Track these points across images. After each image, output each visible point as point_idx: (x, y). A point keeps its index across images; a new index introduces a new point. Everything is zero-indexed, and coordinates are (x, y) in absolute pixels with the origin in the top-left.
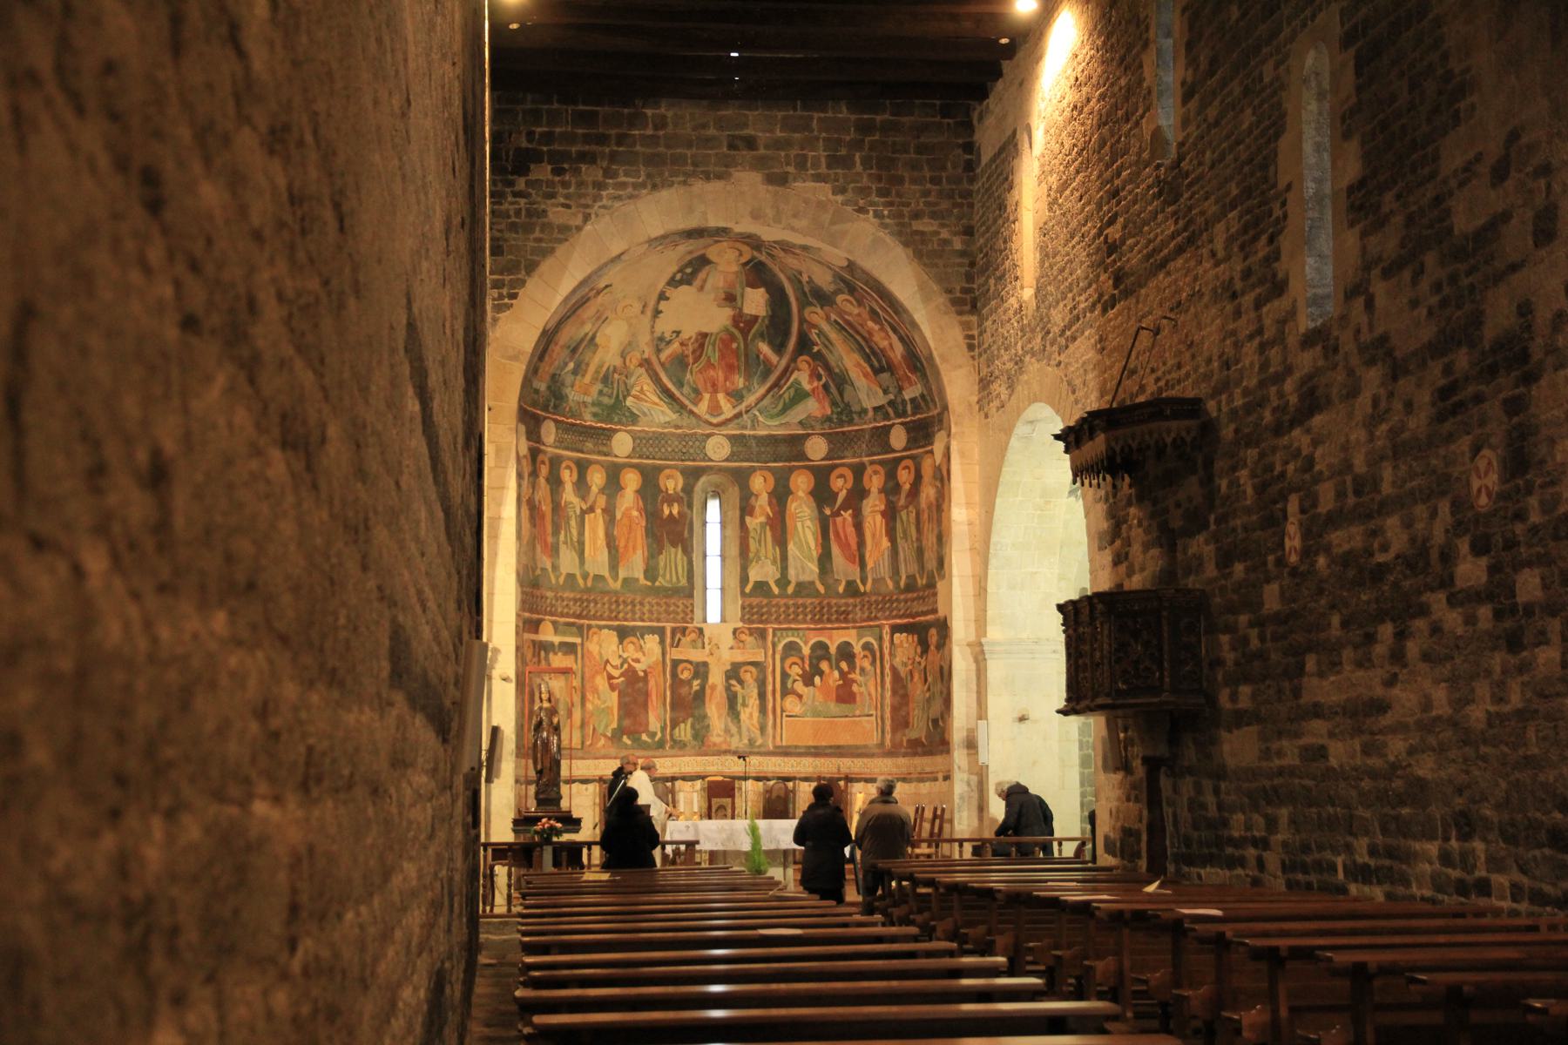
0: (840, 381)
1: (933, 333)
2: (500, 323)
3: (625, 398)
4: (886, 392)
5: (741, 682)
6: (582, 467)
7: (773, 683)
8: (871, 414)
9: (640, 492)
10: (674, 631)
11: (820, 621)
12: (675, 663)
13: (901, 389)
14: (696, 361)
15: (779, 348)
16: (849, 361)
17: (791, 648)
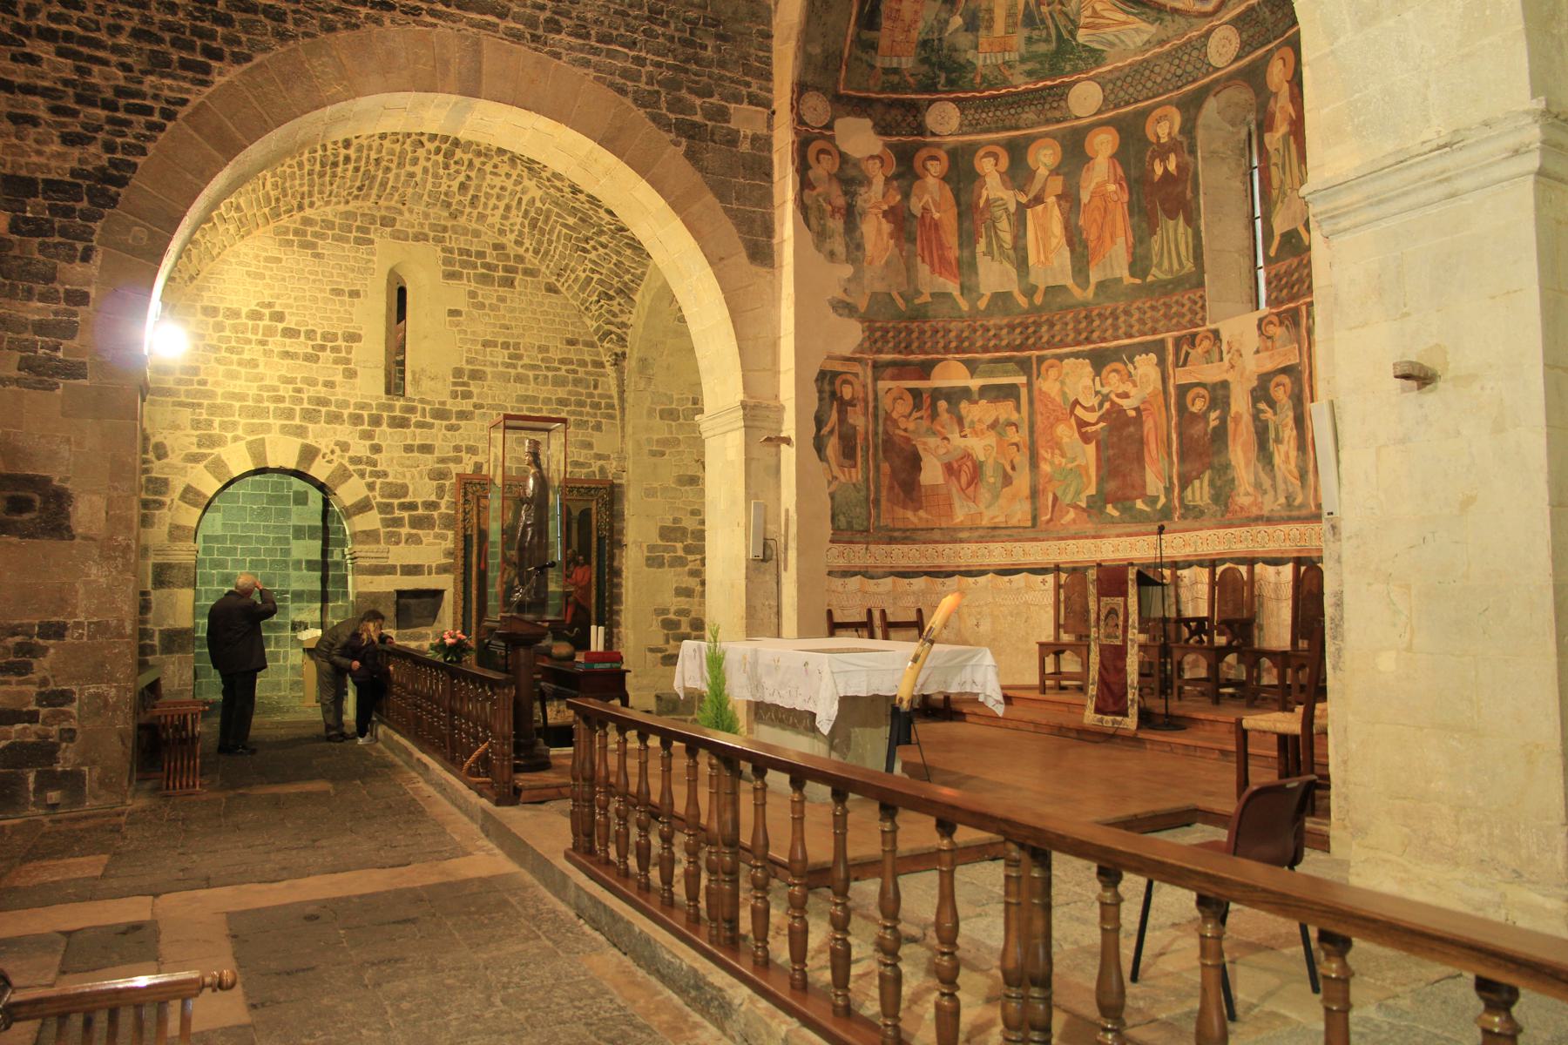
3: (1073, 34)
5: (1272, 404)
6: (1017, 152)
9: (1119, 156)
10: (1178, 343)
12: (1183, 390)
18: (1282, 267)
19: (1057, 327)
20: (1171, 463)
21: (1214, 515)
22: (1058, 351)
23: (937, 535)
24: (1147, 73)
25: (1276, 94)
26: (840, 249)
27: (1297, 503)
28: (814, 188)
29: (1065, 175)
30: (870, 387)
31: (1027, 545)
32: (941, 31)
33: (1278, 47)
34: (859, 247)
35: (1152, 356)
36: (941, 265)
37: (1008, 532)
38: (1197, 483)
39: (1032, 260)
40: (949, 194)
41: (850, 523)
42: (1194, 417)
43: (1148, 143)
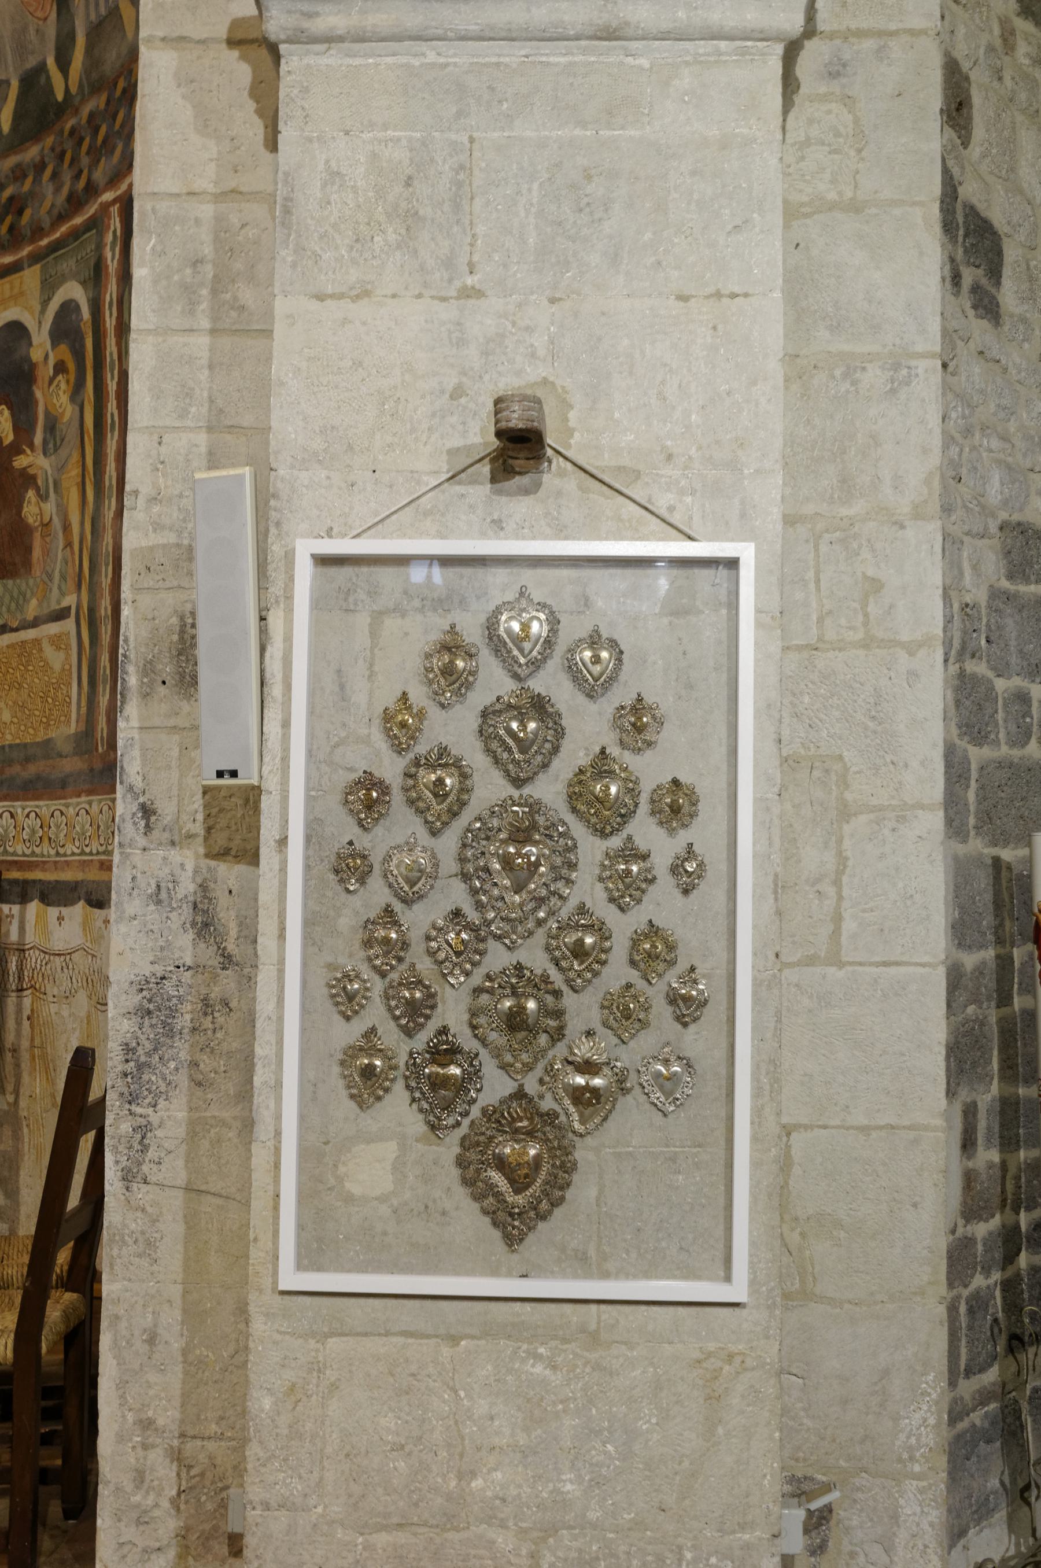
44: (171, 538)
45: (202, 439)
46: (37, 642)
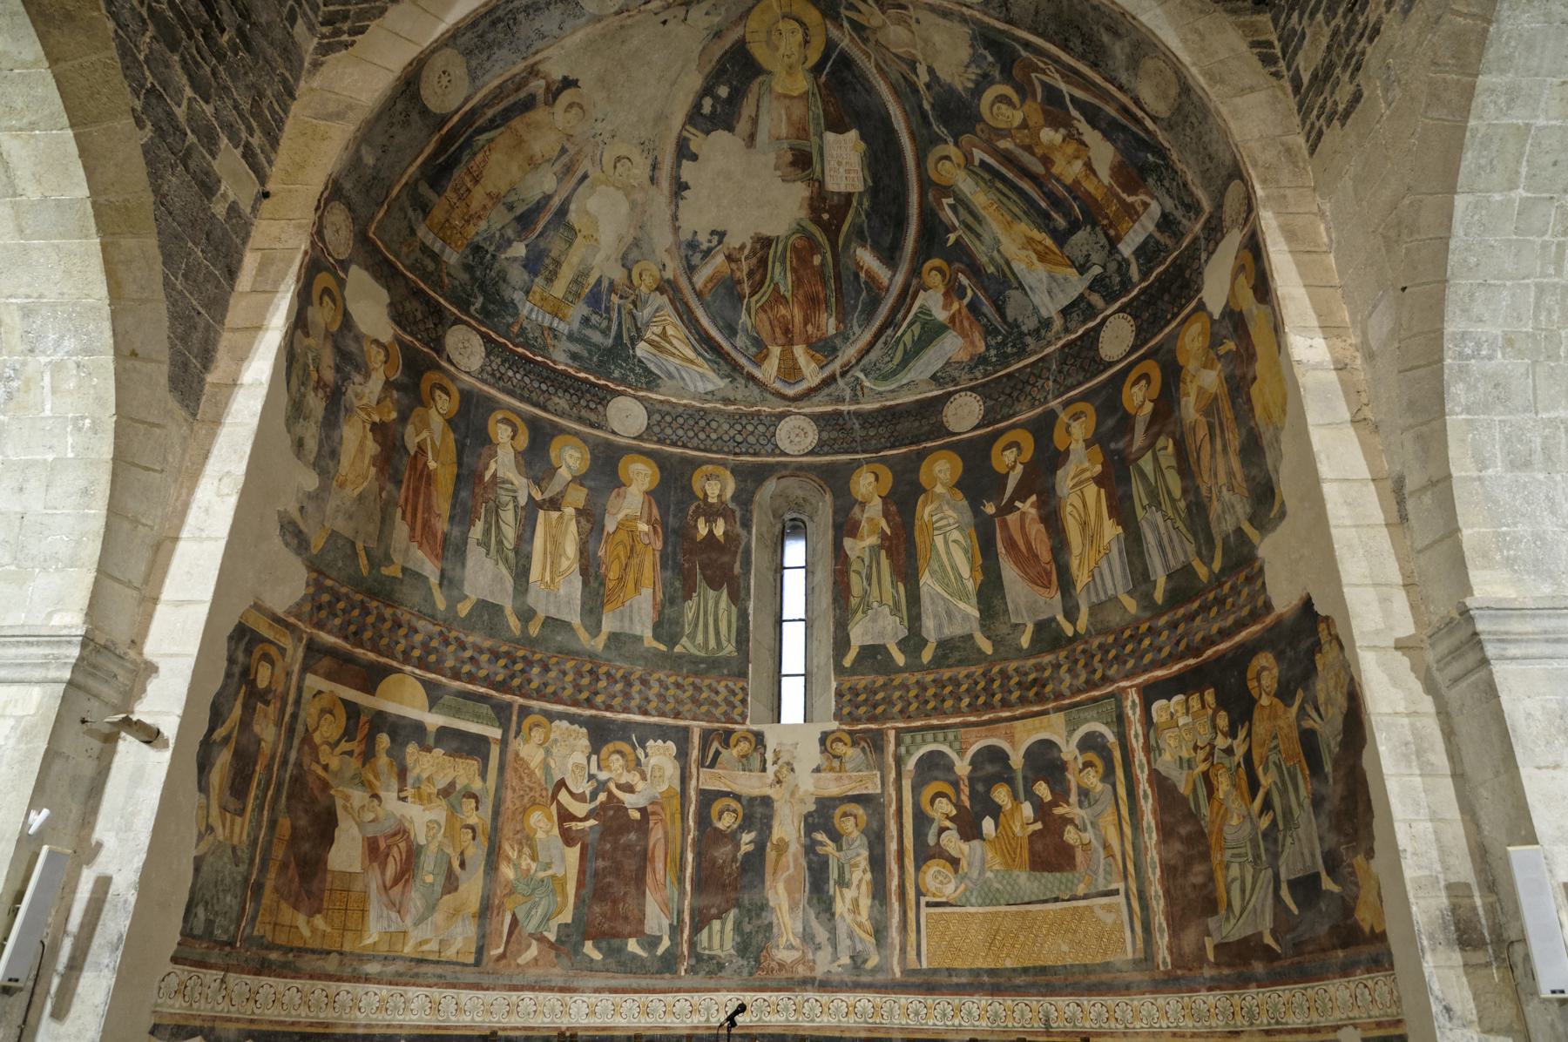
0: (999, 284)
1: (1184, 41)
2: (324, 69)
4: (1082, 269)
5: (836, 837)
7: (899, 836)
8: (1058, 324)
9: (656, 495)
10: (706, 737)
11: (988, 706)
12: (708, 798)
13: (1113, 243)
14: (752, 295)
15: (890, 256)
16: (1009, 240)
17: (933, 765)
18: (862, 681)
19: (552, 674)
20: (682, 893)
21: (738, 971)
22: (549, 706)
23: (331, 965)
24: (702, 423)
25: (863, 504)
26: (312, 445)
27: (870, 965)
28: (307, 335)
29: (590, 489)
30: (295, 678)
31: (465, 996)
32: (499, 248)
33: (868, 461)
34: (334, 454)
35: (670, 744)
36: (423, 532)
37: (439, 970)
38: (716, 924)
39: (534, 575)
40: (452, 445)
41: (210, 923)
42: (720, 836)
43: (694, 497)
44: (1427, 872)
45: (1429, 824)
46: (1090, 908)
